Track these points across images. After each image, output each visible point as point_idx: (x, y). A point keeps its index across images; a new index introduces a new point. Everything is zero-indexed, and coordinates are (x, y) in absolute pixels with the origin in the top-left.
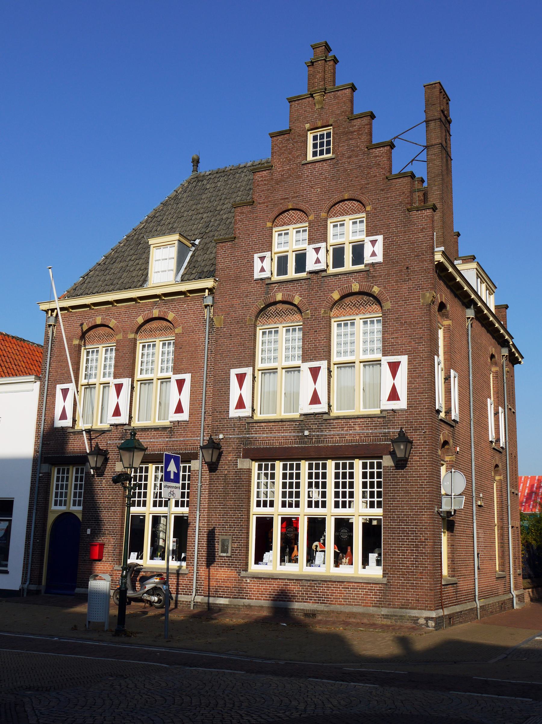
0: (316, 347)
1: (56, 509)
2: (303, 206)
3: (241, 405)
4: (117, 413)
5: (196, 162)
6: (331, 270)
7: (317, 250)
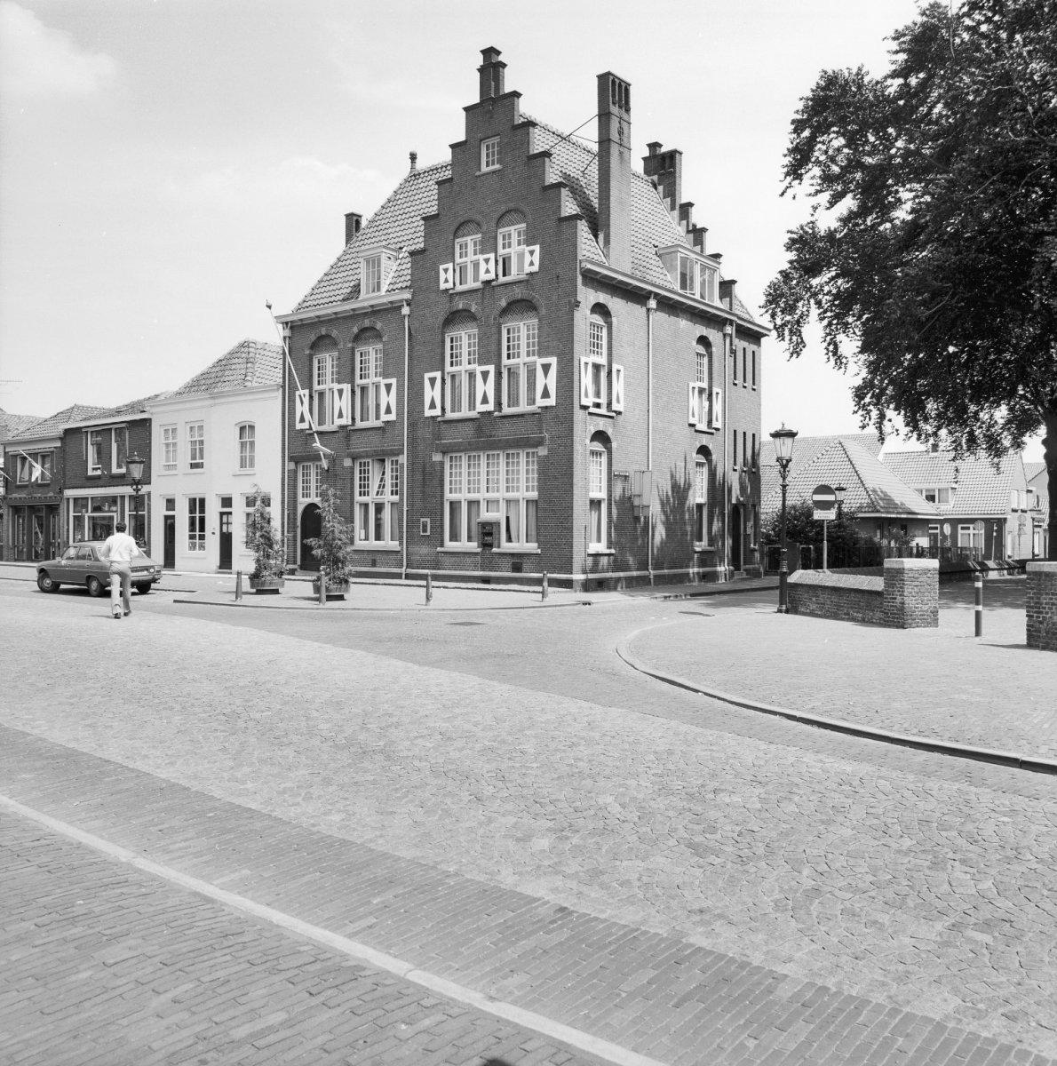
0: (489, 352)
1: (303, 502)
2: (478, 217)
3: (433, 406)
4: (340, 416)
5: (413, 157)
6: (502, 279)
7: (487, 261)
